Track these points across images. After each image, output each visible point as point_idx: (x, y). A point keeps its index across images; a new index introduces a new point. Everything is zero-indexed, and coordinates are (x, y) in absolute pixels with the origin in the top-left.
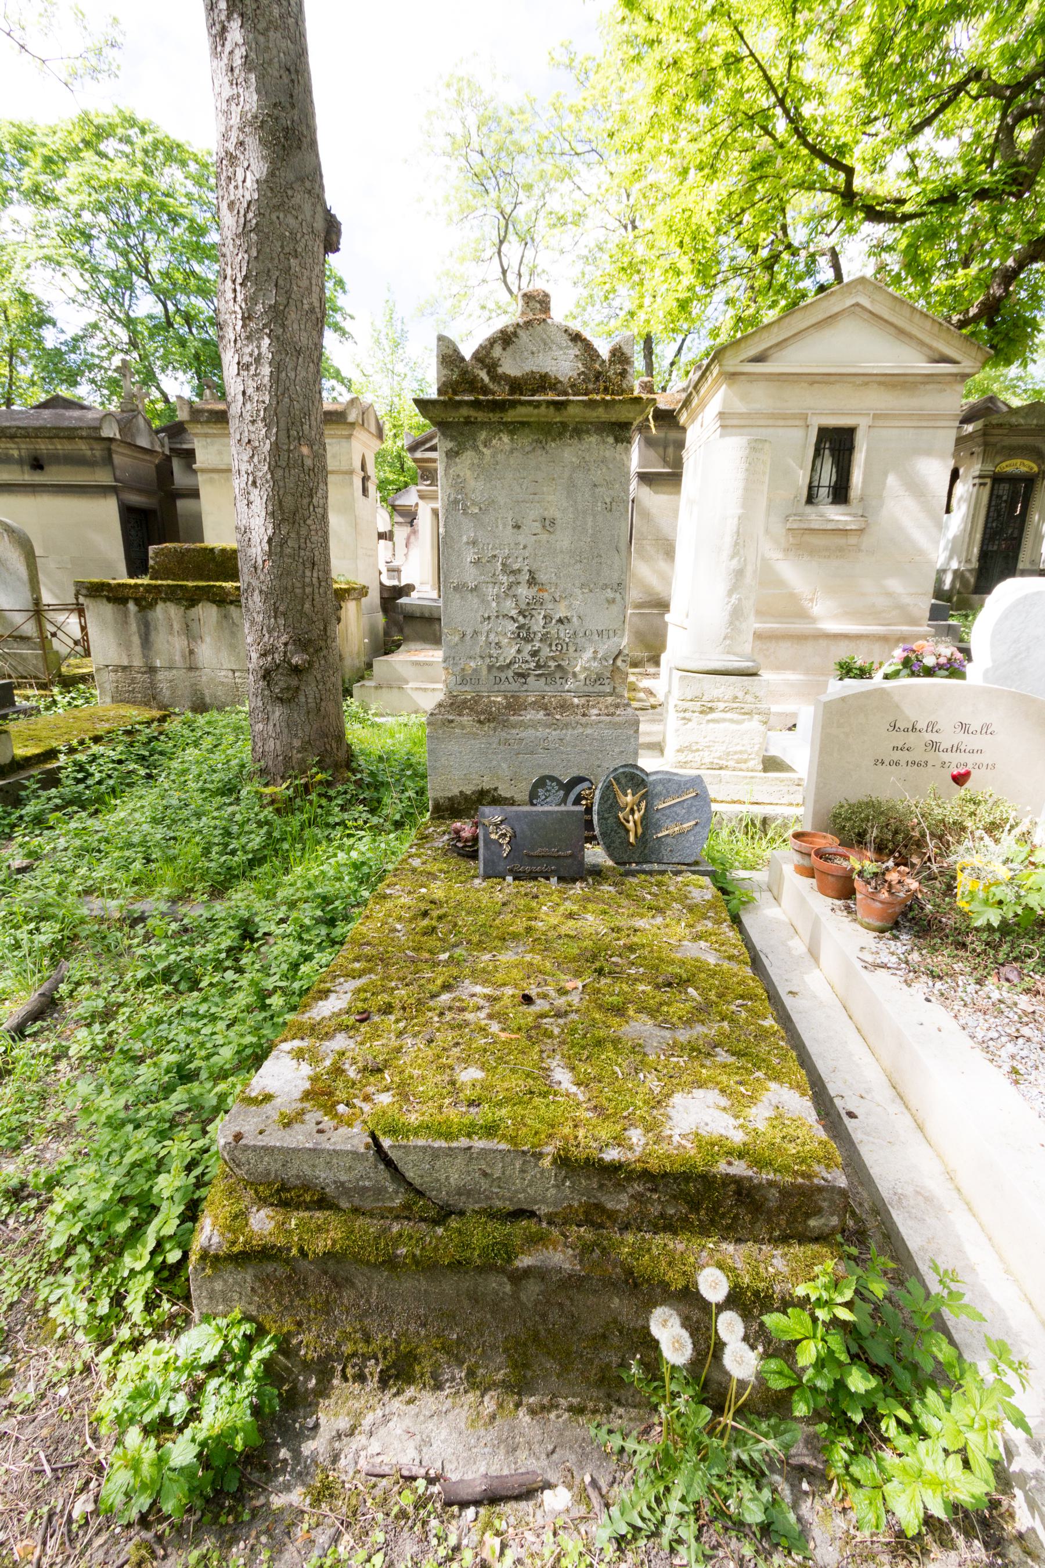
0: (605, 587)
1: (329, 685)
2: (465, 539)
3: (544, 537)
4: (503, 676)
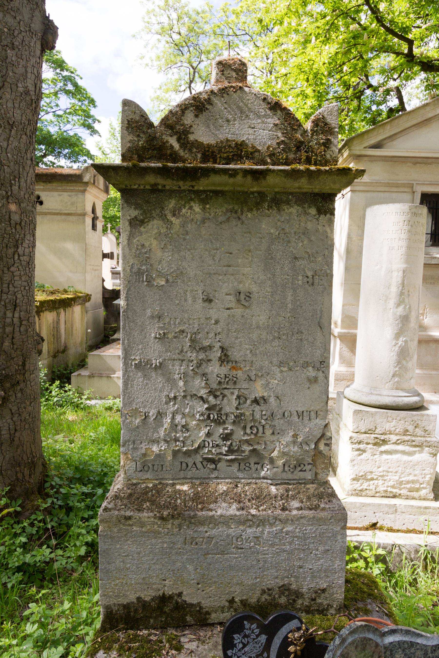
0: (306, 365)
1: (25, 415)
2: (149, 312)
3: (239, 311)
4: (190, 461)
